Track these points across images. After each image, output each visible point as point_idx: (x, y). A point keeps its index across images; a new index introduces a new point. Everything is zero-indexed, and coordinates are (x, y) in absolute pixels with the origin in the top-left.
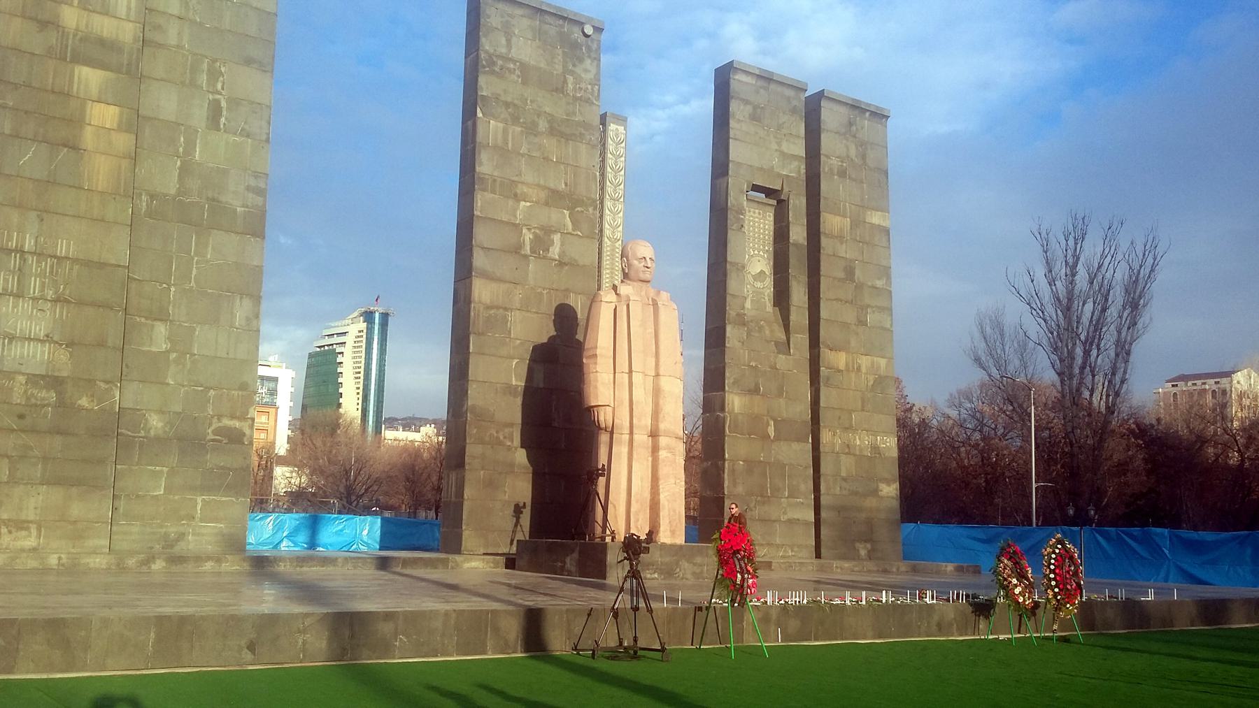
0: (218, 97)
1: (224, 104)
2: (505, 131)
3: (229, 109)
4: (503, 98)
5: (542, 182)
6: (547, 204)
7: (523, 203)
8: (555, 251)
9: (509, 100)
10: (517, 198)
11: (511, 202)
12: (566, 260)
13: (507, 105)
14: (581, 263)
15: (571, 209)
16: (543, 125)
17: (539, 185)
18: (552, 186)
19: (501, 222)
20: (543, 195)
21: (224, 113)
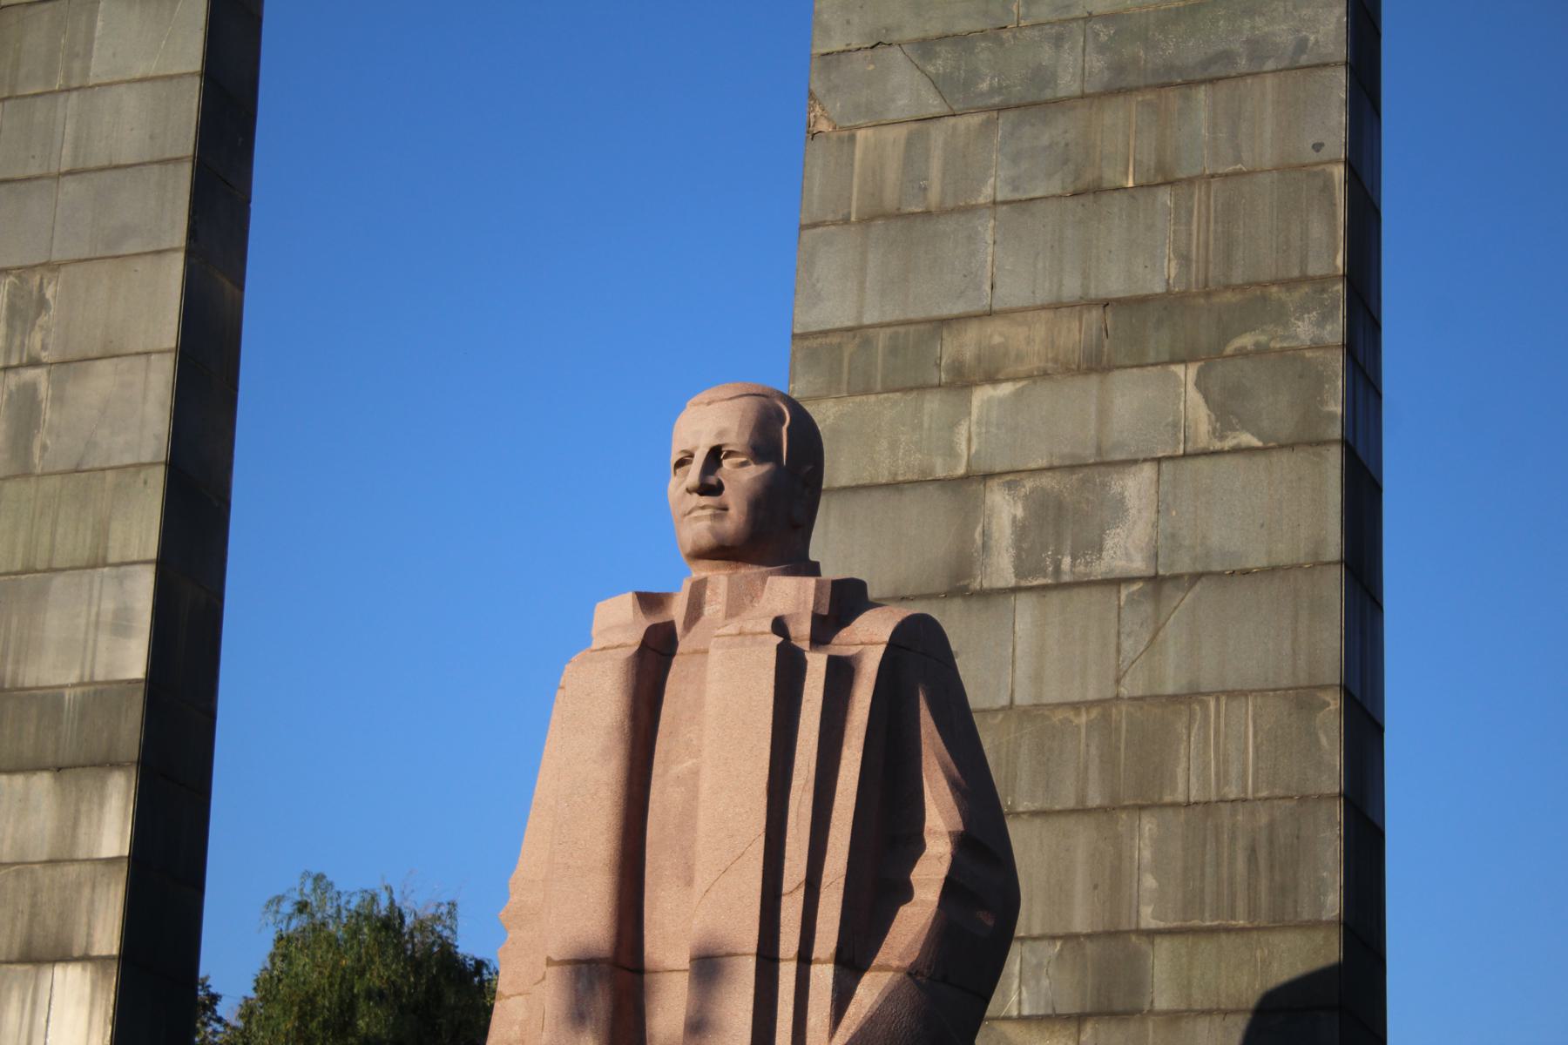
0: (29, 374)
1: (44, 390)
2: (914, 151)
3: (59, 399)
4: (911, 33)
5: (1072, 288)
6: (1095, 364)
7: (982, 395)
8: (1125, 549)
9: (935, 28)
10: (962, 381)
11: (933, 404)
12: (1184, 565)
13: (925, 47)
14: (1257, 560)
15: (1206, 356)
16: (1073, 69)
17: (1056, 306)
18: (1115, 285)
19: (894, 486)
20: (1073, 334)
21: (48, 414)
